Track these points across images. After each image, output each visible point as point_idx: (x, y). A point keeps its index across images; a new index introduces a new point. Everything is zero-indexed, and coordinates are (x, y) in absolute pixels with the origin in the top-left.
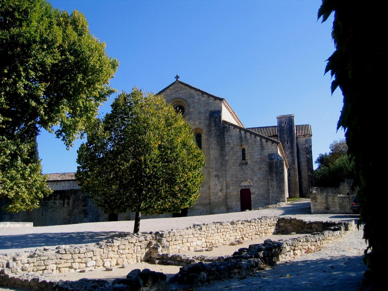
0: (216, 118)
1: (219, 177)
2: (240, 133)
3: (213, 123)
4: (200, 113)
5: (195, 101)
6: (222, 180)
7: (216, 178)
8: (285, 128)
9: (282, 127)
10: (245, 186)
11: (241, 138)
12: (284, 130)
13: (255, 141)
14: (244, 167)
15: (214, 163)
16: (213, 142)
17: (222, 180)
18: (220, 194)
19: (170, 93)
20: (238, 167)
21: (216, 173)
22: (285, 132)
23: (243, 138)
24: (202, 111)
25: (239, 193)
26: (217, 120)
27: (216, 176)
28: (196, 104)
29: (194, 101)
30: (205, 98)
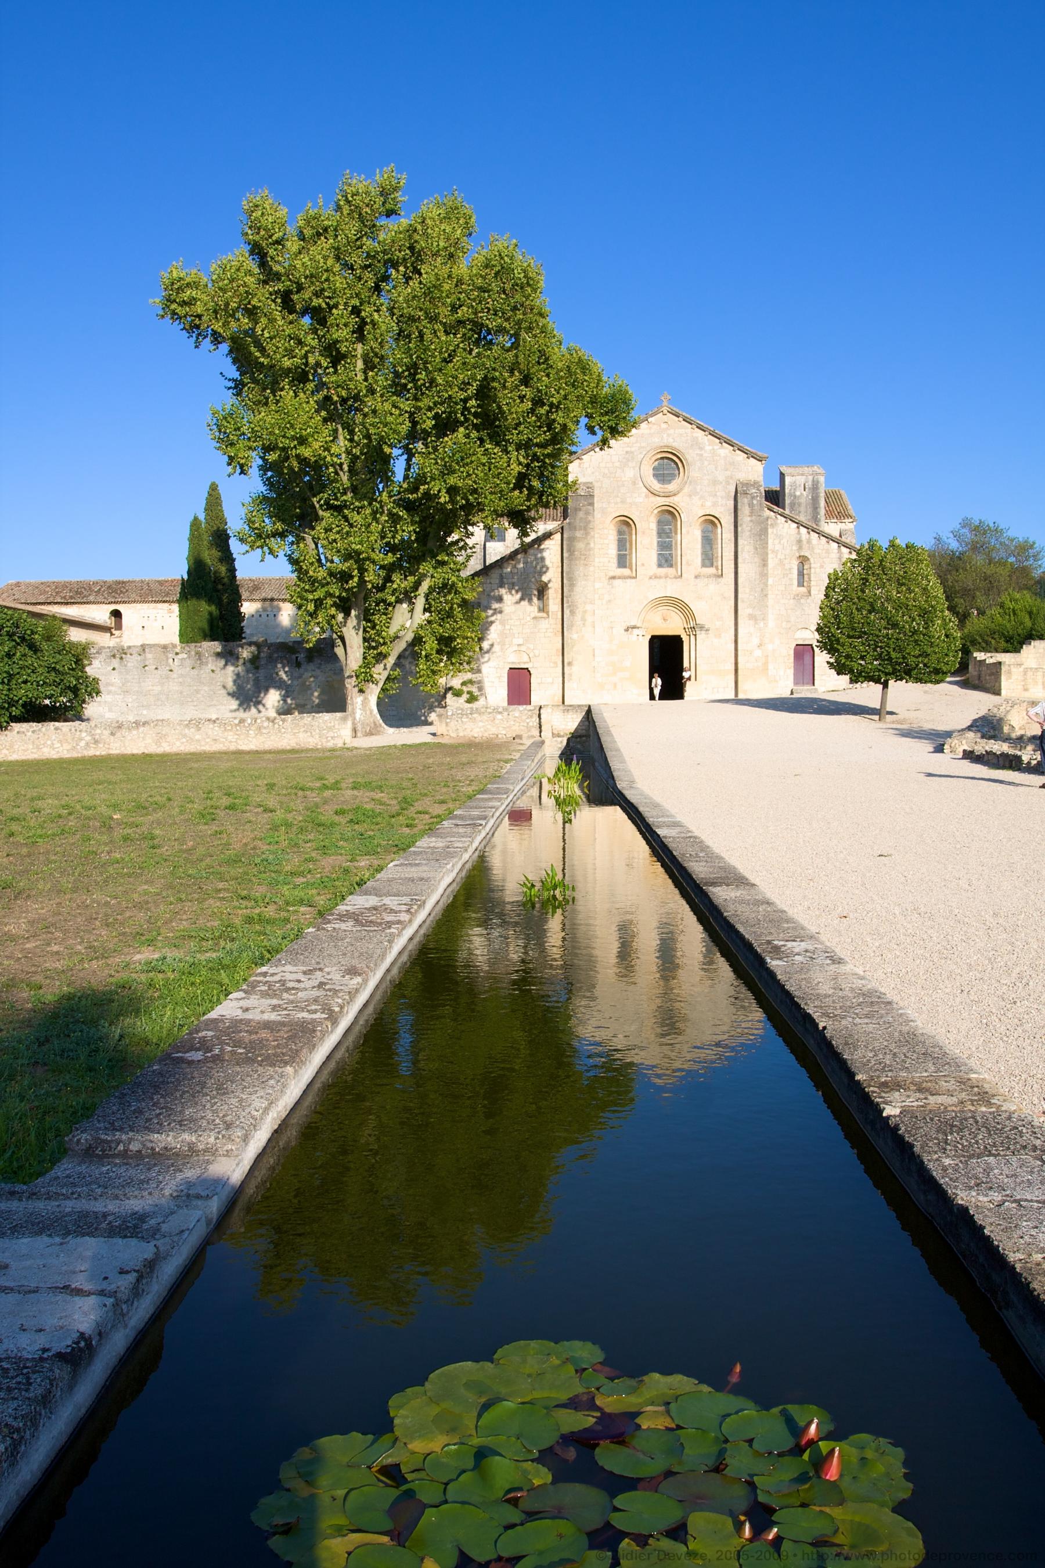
0: (753, 498)
1: (756, 620)
2: (799, 533)
3: (747, 507)
4: (715, 482)
5: (705, 455)
6: (762, 625)
7: (752, 622)
8: (803, 501)
9: (795, 496)
10: (805, 640)
11: (800, 541)
12: (799, 505)
13: (828, 552)
14: (802, 601)
15: (747, 590)
16: (747, 548)
17: (762, 625)
18: (758, 653)
19: (648, 431)
20: (792, 601)
21: (750, 611)
22: (802, 509)
23: (805, 542)
24: (721, 478)
25: (792, 652)
26: (755, 502)
27: (752, 617)
28: (706, 463)
29: (702, 455)
30: (727, 451)
